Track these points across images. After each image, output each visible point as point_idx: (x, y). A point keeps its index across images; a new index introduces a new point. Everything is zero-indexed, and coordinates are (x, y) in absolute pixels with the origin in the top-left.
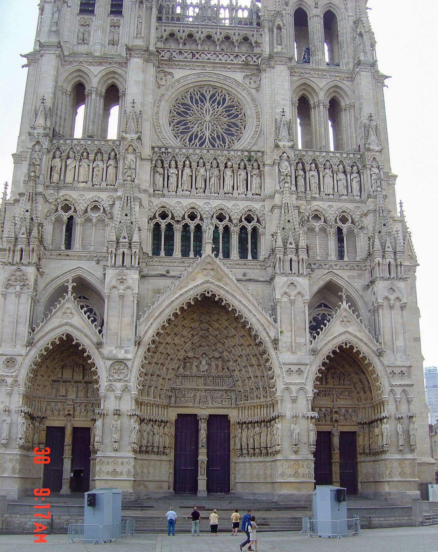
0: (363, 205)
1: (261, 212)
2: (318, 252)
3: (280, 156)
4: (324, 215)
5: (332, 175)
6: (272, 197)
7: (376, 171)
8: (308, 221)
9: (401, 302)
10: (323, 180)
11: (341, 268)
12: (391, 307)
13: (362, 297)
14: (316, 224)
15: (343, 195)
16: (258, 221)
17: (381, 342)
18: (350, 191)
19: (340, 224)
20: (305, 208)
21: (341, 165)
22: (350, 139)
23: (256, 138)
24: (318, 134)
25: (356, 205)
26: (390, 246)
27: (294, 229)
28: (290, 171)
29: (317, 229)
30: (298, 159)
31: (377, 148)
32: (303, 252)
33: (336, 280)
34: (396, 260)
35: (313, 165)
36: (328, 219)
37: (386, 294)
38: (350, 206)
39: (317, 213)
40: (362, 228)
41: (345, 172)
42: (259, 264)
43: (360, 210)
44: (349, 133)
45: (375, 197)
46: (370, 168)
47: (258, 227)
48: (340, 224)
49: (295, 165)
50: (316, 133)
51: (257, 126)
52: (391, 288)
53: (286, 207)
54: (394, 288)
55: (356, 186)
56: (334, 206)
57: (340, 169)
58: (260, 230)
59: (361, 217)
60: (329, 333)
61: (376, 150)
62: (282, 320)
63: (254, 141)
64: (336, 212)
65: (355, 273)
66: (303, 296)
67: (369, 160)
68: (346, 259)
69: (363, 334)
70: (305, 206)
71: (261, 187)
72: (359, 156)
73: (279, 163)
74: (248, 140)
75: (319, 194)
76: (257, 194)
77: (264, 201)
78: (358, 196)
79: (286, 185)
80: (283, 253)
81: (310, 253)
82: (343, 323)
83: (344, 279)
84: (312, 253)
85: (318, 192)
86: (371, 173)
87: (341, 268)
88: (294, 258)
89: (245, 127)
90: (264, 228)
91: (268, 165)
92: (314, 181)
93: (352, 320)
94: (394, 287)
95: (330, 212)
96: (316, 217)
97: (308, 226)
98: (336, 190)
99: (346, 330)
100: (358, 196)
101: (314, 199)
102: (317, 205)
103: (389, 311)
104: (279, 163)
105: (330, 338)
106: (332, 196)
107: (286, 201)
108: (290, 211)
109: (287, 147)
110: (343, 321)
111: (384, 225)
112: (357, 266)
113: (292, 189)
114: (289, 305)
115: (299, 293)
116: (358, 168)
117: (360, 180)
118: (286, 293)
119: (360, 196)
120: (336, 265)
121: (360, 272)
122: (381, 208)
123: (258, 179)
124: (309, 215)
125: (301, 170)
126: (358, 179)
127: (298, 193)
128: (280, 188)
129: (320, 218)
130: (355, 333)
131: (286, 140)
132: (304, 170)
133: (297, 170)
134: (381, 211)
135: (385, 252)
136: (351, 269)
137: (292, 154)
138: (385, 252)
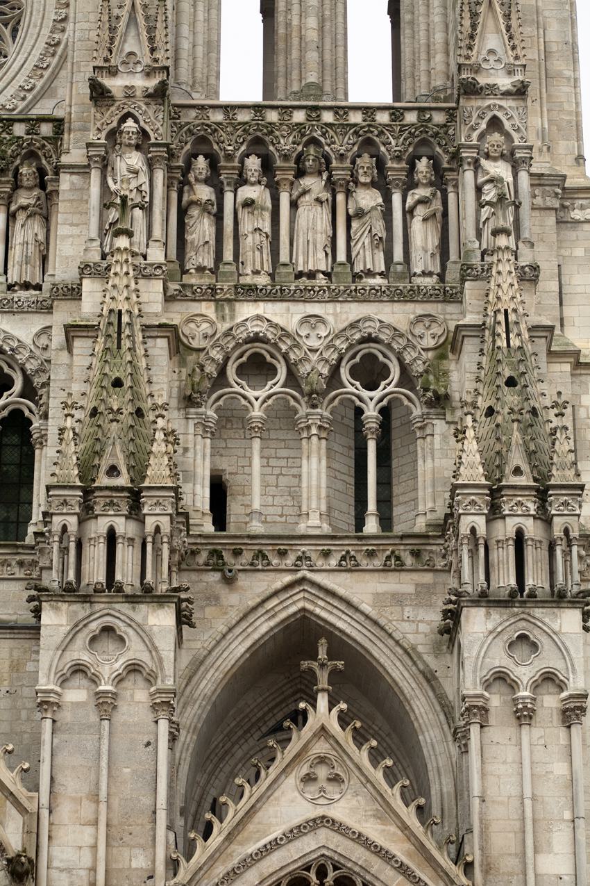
0: (451, 308)
1: (38, 352)
2: (256, 505)
3: (113, 135)
4: (285, 357)
5: (326, 195)
6: (73, 293)
7: (501, 170)
8: (221, 379)
9: (564, 694)
10: (292, 221)
11: (349, 565)
12: (524, 716)
13: (428, 681)
14: (251, 394)
15: (370, 273)
16: (29, 391)
17: (469, 859)
18: (398, 255)
19: (351, 387)
20: (210, 332)
21: (366, 156)
22: (423, 56)
23: (50, 70)
24: (295, 41)
25: (420, 309)
26: (525, 467)
27: (139, 413)
28: (146, 188)
29: (257, 412)
30: (191, 139)
31: (505, 82)
32: (158, 504)
33: (324, 614)
34: (547, 521)
35: (253, 163)
36: (304, 369)
37: (499, 658)
38: (396, 315)
39: (260, 348)
40: (440, 402)
41: (382, 184)
42: (18, 558)
43: (437, 330)
44: (422, 34)
45: (484, 275)
46: (476, 161)
47: (27, 413)
48: (352, 389)
49: (180, 163)
50: (288, 37)
51: (59, 26)
52: (523, 637)
53: (113, 331)
54: (535, 635)
55: (423, 236)
56: (330, 319)
57: (361, 171)
58: (36, 423)
59: (443, 357)
60: (251, 827)
61: (504, 89)
62: (60, 778)
63: (42, 81)
64: (337, 343)
65: (404, 584)
66: (150, 679)
67: (473, 129)
68: (372, 526)
69: (393, 829)
70: (212, 323)
71: (44, 259)
72: (439, 118)
73: (104, 159)
74: (21, 80)
75: (272, 276)
76: (26, 286)
77: (49, 310)
78: (430, 274)
79: (122, 242)
80: (77, 510)
81: (234, 509)
82: (312, 789)
83: (357, 609)
84: (242, 510)
85: (267, 267)
86: (481, 180)
87: (348, 564)
88: (123, 526)
89: (15, 31)
90: (45, 416)
91: (73, 169)
92: (254, 225)
93: (348, 771)
94: (536, 632)
95: (313, 343)
96: (257, 368)
97: (221, 402)
98: (341, 257)
99: (320, 812)
100: (430, 274)
101: (251, 293)
102: (259, 318)
103: (511, 730)
104: (104, 159)
105: (252, 848)
106: (321, 280)
107: (113, 306)
108: (126, 344)
109: (139, 93)
110: (309, 779)
111: (511, 382)
112: (416, 554)
113: (150, 259)
114: (94, 718)
115: (134, 669)
116: (436, 166)
117: (445, 214)
118: (79, 669)
119: (442, 277)
120: (326, 554)
121: (428, 578)
122: (501, 318)
123: (36, 227)
124: (227, 359)
125: (207, 182)
126: (437, 205)
127: (185, 272)
128: (104, 257)
129: (272, 371)
130: (357, 827)
131: (139, 69)
132: (213, 179)
133: (189, 183)
134: (501, 329)
135: (500, 489)
136: (386, 570)
137: (156, 123)
138: (500, 489)
